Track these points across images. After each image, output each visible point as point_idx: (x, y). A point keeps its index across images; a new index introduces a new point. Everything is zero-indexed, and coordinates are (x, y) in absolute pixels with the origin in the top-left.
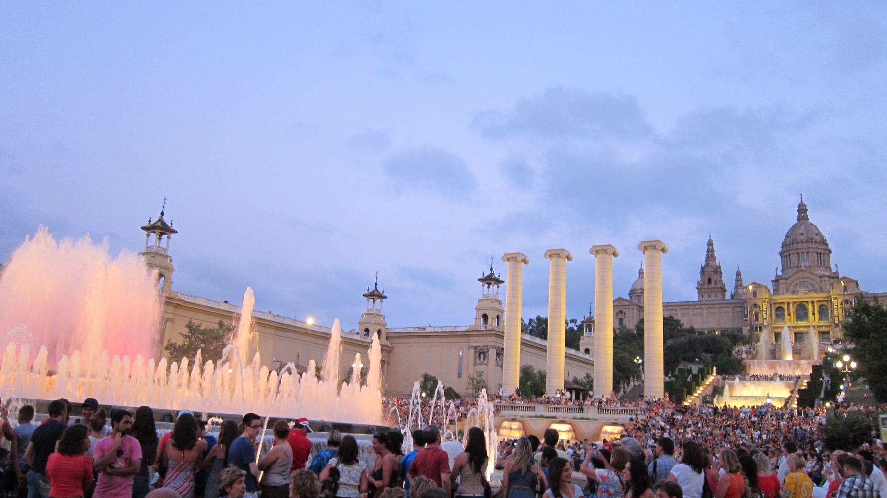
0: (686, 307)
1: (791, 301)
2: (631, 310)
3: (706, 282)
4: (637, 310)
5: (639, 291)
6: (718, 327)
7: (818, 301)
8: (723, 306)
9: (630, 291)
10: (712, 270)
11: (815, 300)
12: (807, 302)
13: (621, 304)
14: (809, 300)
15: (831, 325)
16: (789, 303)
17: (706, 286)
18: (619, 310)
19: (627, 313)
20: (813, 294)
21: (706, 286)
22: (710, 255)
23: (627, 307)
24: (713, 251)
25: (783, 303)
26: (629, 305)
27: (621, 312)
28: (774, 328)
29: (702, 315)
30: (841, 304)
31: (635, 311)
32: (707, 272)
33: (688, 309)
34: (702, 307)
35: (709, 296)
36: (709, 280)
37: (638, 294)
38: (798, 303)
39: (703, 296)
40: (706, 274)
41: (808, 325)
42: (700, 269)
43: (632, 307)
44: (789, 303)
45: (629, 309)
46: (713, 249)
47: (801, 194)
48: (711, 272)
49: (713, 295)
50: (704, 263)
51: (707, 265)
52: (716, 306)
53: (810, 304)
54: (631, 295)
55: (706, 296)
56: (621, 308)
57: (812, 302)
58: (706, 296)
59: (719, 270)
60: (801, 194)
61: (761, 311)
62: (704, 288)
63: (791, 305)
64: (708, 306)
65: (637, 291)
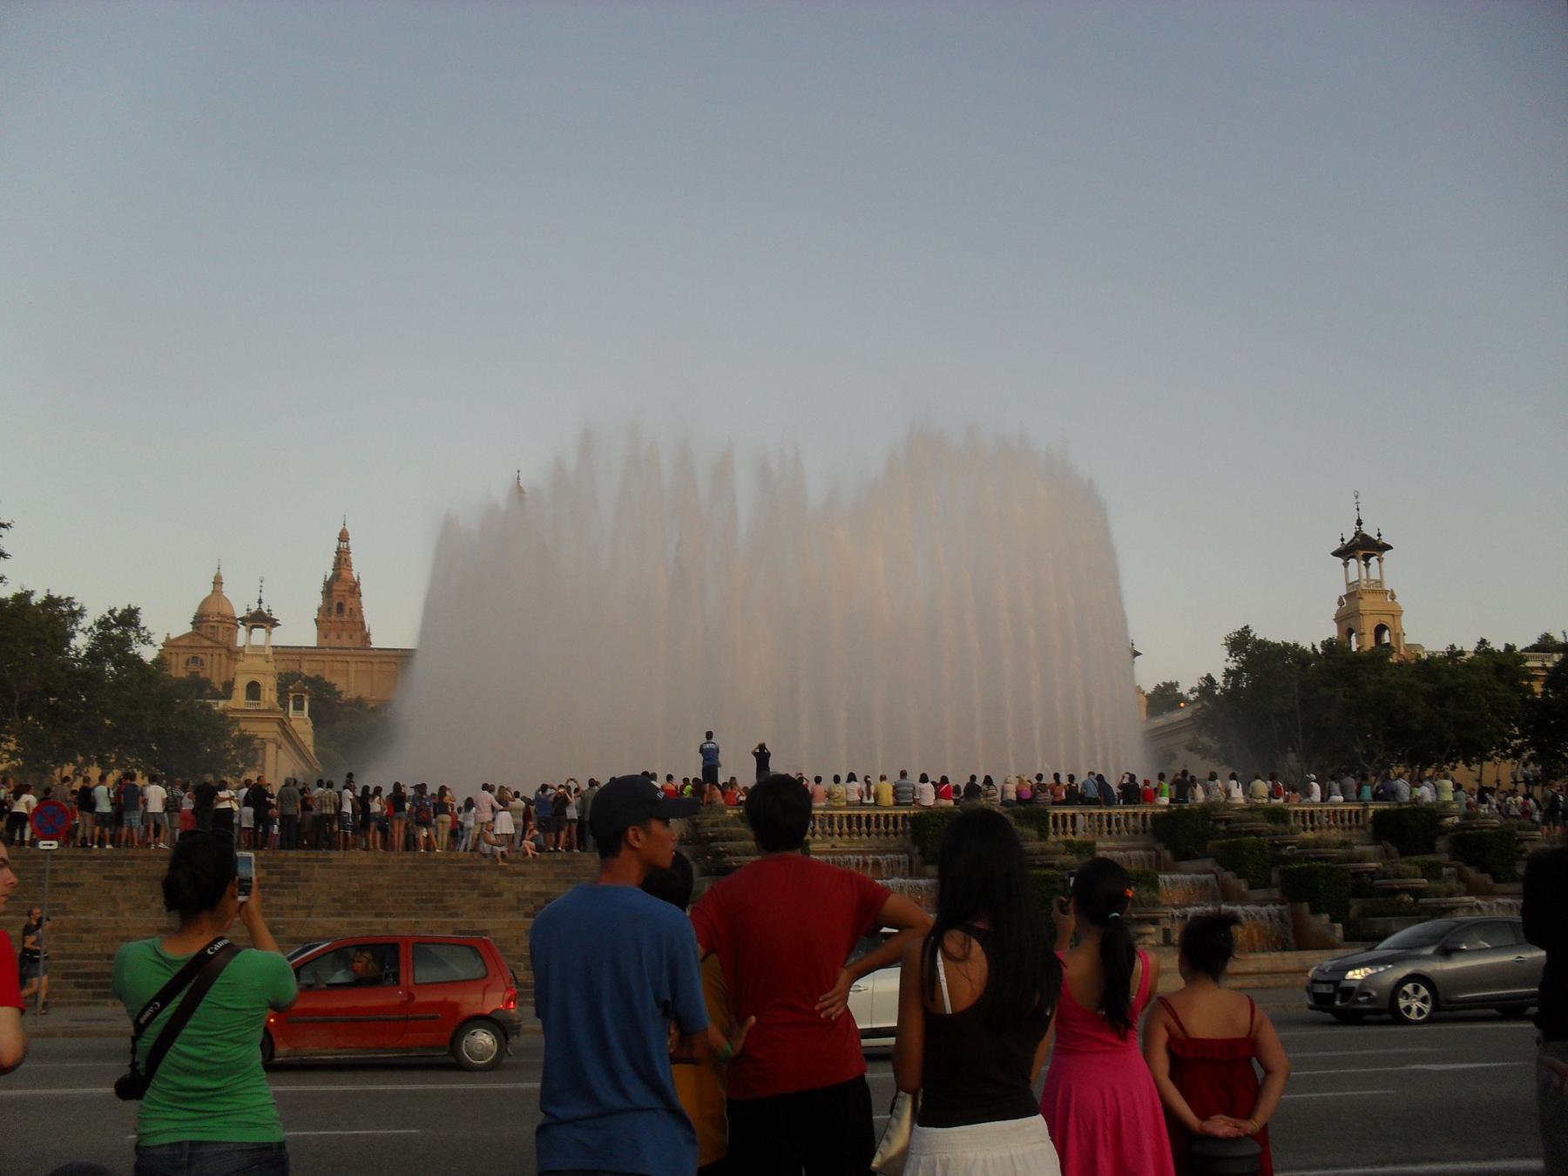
0: (318, 658)
2: (216, 658)
3: (334, 609)
4: (226, 656)
5: (216, 618)
6: (374, 697)
8: (386, 659)
9: (195, 617)
10: (347, 588)
13: (196, 644)
17: (333, 618)
18: (191, 655)
19: (207, 660)
21: (333, 618)
22: (343, 560)
23: (209, 651)
24: (347, 551)
26: (212, 647)
27: (195, 659)
29: (348, 675)
31: (223, 657)
32: (336, 591)
33: (323, 661)
34: (348, 659)
35: (339, 637)
36: (340, 607)
37: (216, 624)
39: (326, 638)
40: (334, 594)
42: (320, 587)
43: (218, 651)
45: (212, 655)
46: (348, 549)
47: (519, 471)
48: (345, 591)
49: (345, 635)
50: (330, 573)
51: (337, 576)
52: (373, 660)
54: (199, 625)
55: (333, 635)
56: (195, 651)
58: (333, 635)
59: (357, 589)
60: (519, 471)
62: (330, 622)
64: (360, 659)
65: (211, 619)
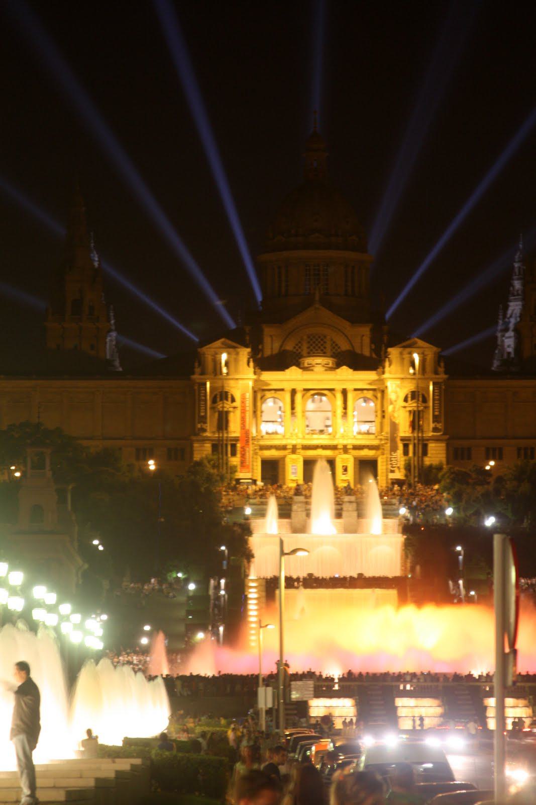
1: (299, 387)
7: (356, 390)
11: (350, 387)
12: (331, 390)
14: (339, 387)
15: (382, 445)
16: (294, 392)
20: (345, 372)
25: (282, 390)
28: (263, 448)
30: (406, 400)
38: (312, 392)
41: (334, 442)
44: (294, 392)
53: (339, 397)
57: (344, 392)
61: (235, 408)
63: (298, 397)
